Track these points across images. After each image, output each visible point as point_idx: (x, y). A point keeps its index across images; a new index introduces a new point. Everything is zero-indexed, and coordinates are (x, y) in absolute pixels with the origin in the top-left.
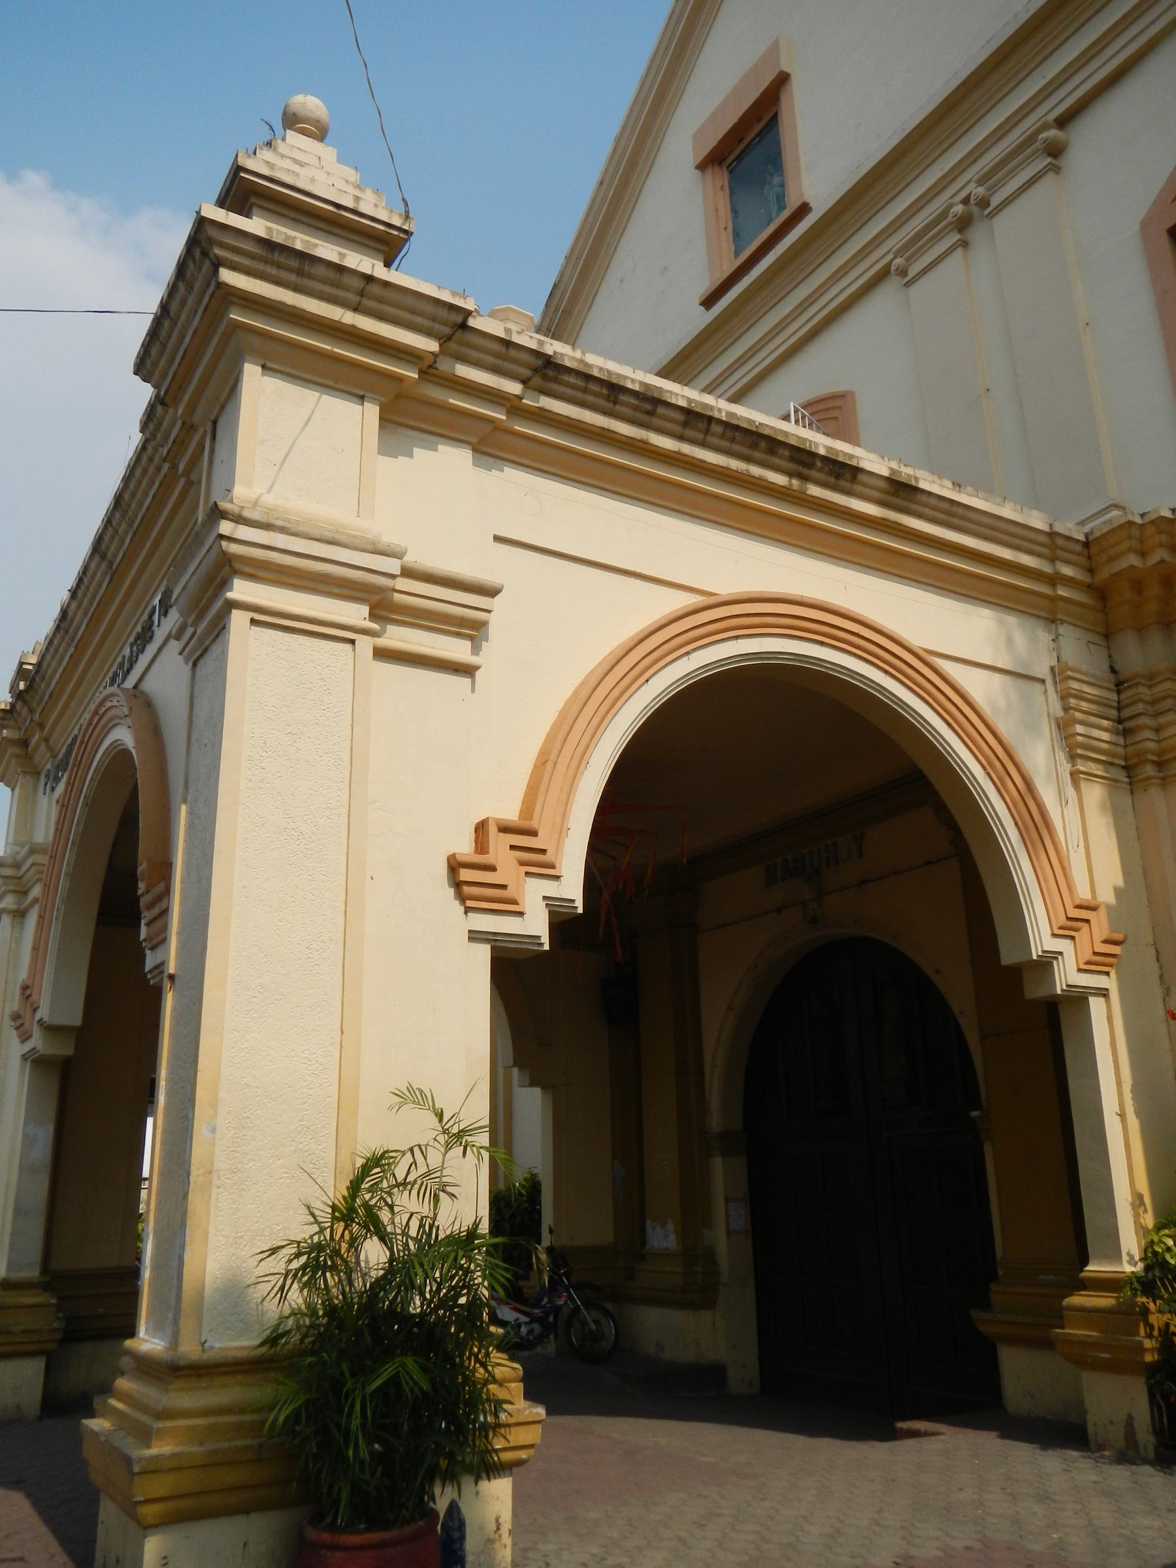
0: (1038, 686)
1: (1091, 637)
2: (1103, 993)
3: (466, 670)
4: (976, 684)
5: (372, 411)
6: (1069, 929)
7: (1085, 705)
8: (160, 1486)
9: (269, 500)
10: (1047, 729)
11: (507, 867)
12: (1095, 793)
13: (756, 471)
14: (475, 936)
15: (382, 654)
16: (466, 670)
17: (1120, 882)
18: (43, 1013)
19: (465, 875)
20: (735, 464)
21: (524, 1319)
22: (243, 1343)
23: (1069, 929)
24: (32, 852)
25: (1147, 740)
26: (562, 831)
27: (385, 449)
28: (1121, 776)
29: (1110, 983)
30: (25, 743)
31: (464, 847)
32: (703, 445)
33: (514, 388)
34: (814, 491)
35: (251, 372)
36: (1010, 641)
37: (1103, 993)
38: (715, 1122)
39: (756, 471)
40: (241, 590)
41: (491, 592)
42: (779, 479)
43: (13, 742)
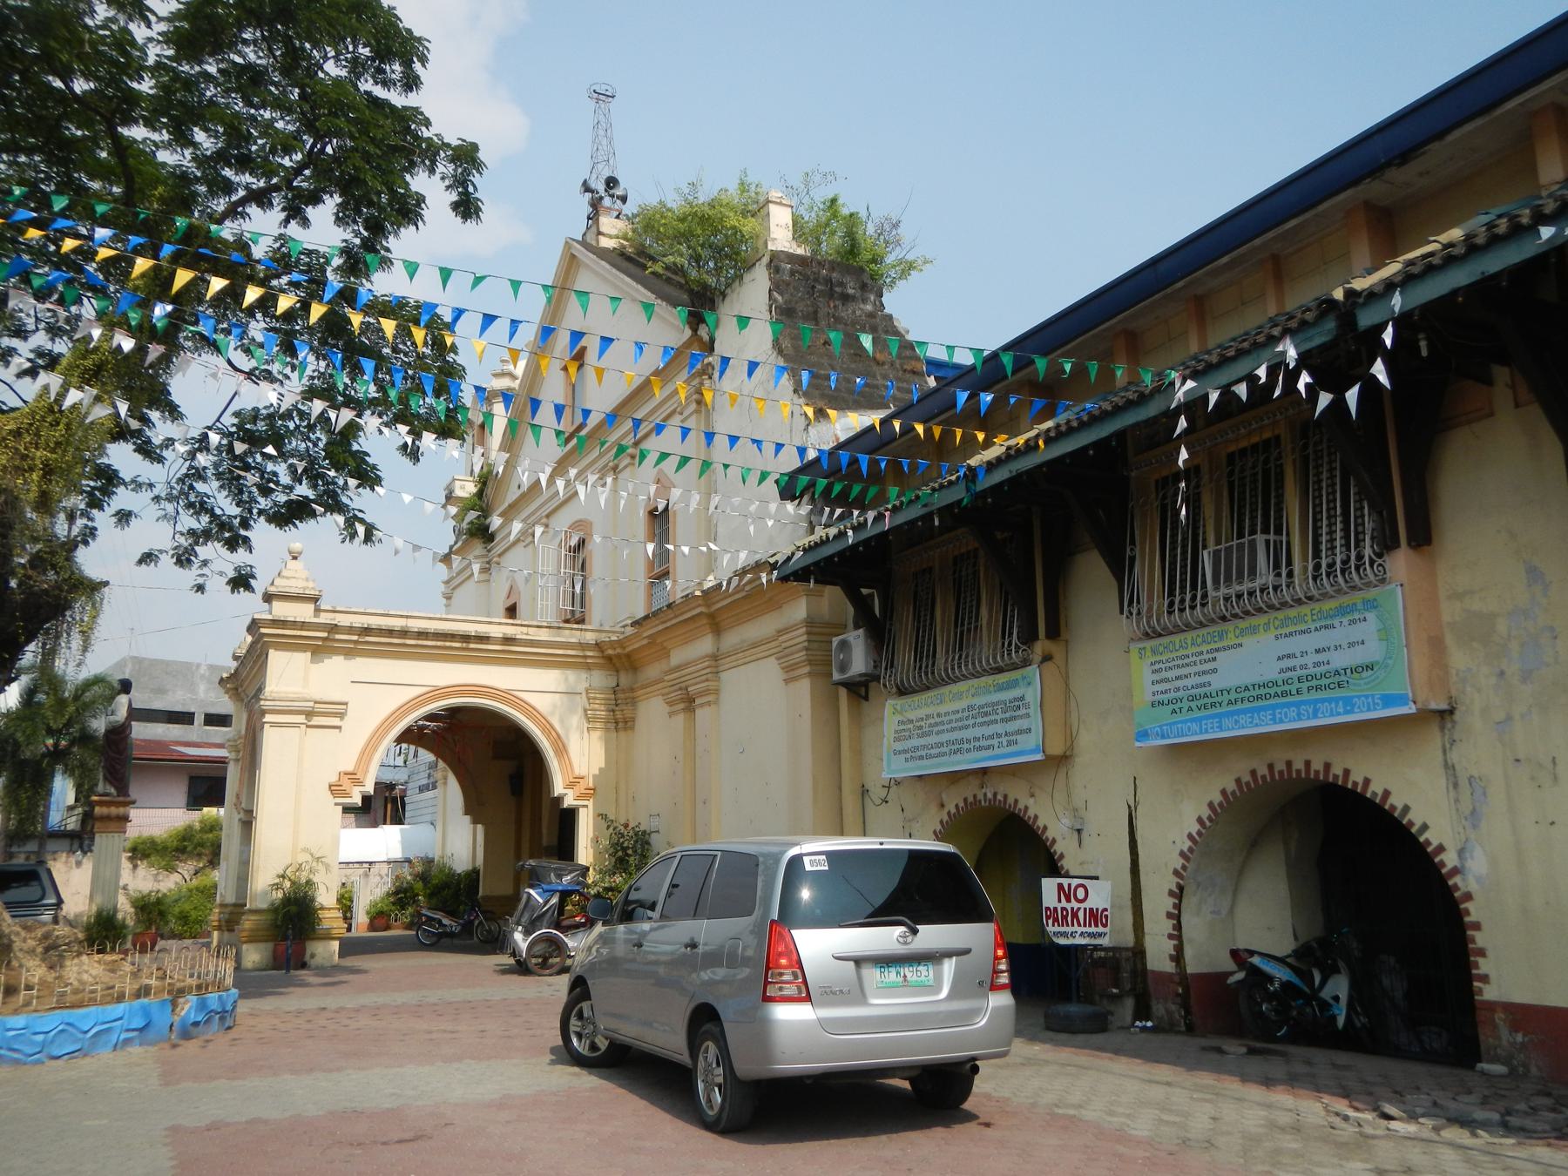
0: (578, 697)
1: (609, 673)
2: (586, 806)
3: (339, 728)
4: (541, 703)
5: (309, 654)
6: (571, 785)
7: (598, 701)
8: (245, 934)
9: (276, 690)
10: (580, 711)
11: (346, 784)
12: (596, 735)
13: (448, 644)
14: (336, 804)
15: (308, 726)
16: (339, 728)
17: (603, 766)
18: (243, 805)
19: (333, 788)
20: (439, 643)
21: (453, 923)
22: (264, 906)
23: (571, 785)
24: (240, 738)
25: (619, 715)
26: (366, 771)
27: (312, 662)
28: (612, 726)
29: (590, 803)
30: (237, 689)
31: (334, 779)
32: (426, 640)
33: (355, 638)
34: (472, 646)
35: (271, 652)
36: (566, 679)
37: (586, 806)
38: (545, 842)
39: (448, 644)
40: (268, 718)
41: (346, 704)
42: (458, 645)
43: (232, 689)
